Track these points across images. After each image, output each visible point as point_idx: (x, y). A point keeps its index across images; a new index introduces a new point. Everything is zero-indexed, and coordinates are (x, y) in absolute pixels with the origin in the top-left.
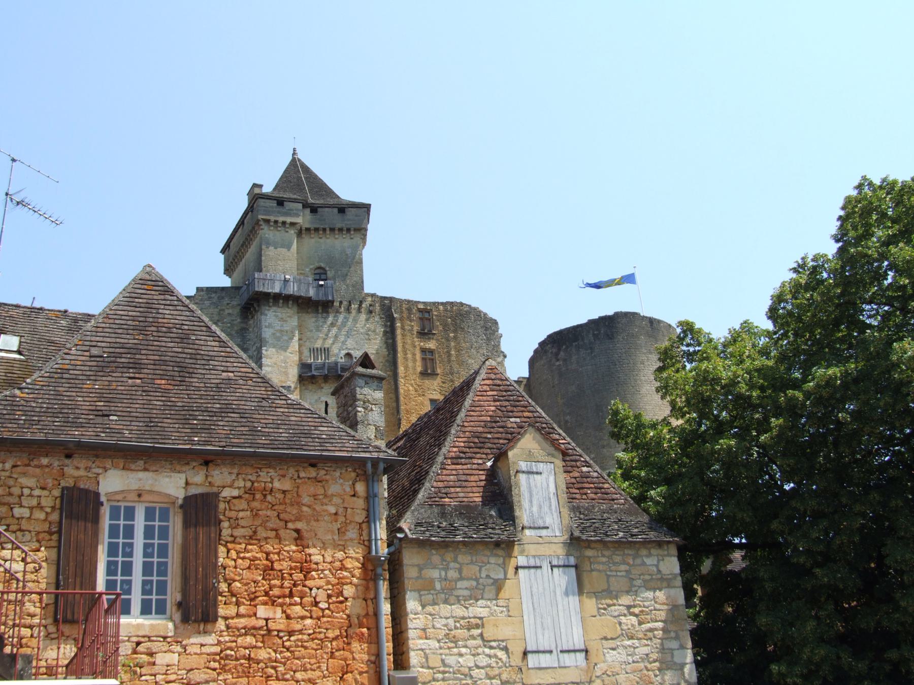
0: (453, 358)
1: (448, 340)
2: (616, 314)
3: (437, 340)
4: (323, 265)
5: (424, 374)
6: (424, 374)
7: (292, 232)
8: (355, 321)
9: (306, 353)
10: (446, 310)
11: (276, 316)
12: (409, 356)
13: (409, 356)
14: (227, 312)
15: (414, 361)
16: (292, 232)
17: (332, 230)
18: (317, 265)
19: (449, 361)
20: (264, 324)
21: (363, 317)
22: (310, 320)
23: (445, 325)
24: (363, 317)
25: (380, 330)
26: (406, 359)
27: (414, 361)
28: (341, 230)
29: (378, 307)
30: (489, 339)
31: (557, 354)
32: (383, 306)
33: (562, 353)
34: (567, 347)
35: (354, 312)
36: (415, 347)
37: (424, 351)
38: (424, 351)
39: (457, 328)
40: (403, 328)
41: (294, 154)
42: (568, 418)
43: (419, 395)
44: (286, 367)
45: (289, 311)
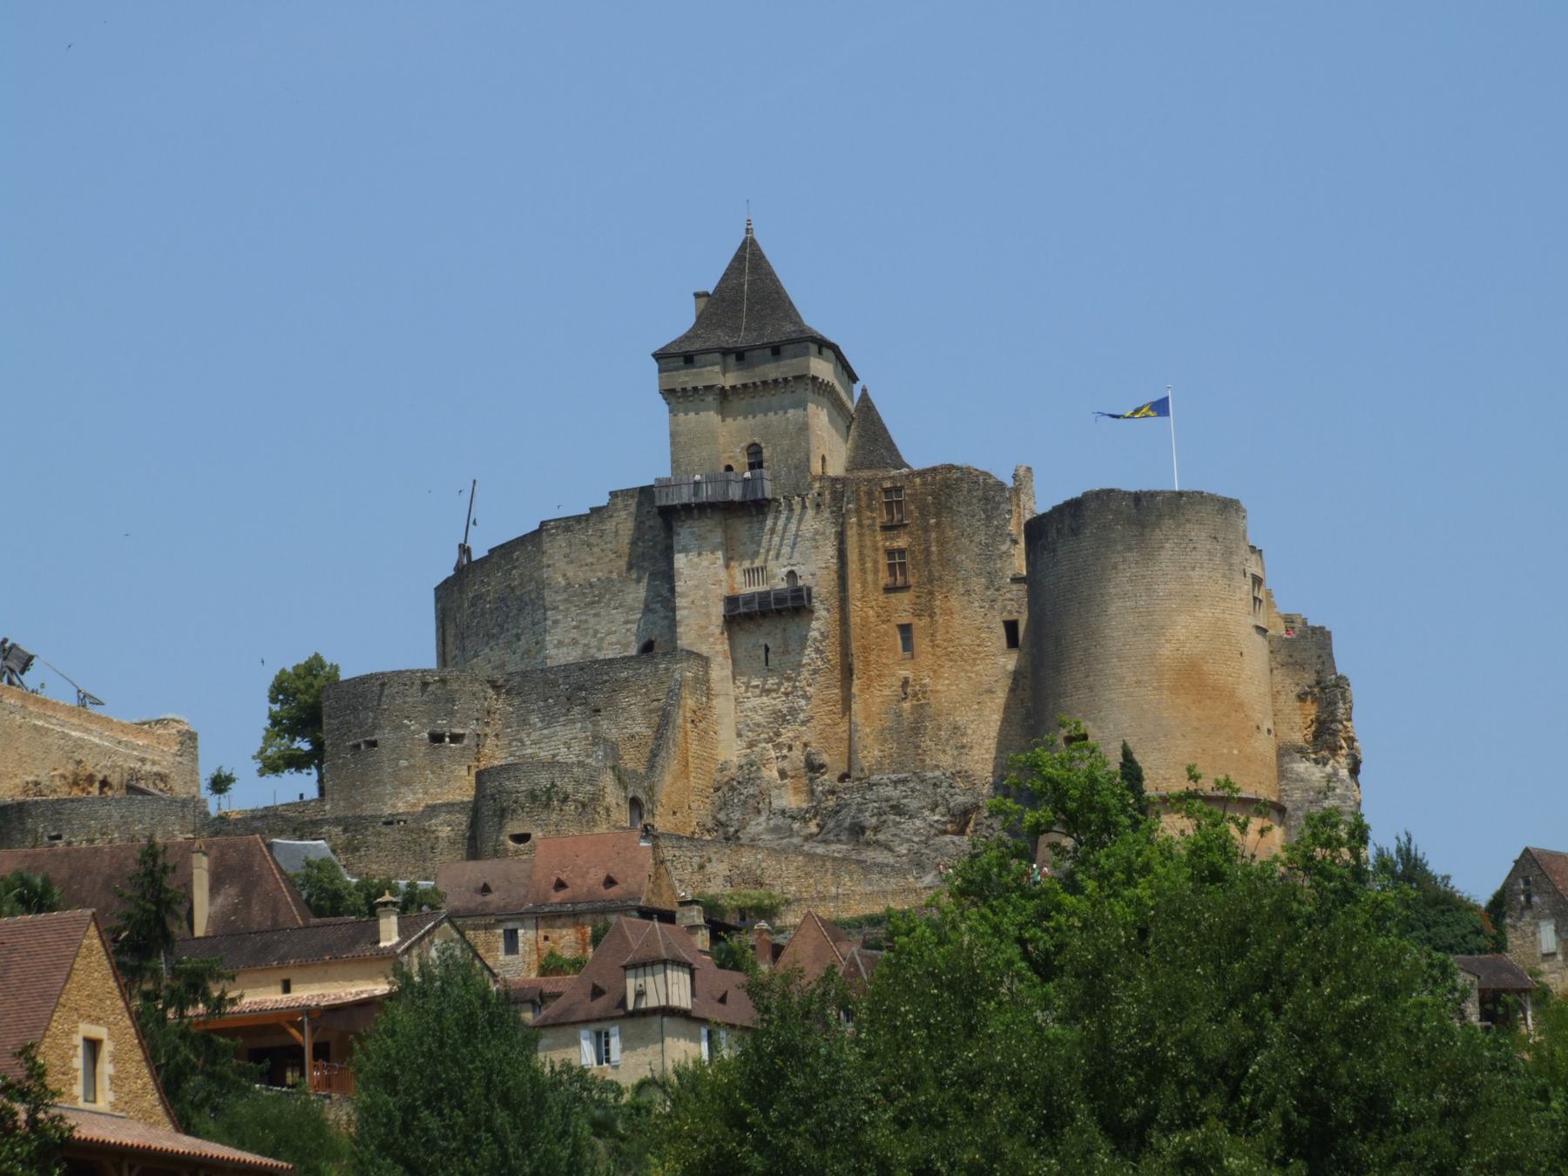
0: (934, 558)
2: (1085, 495)
3: (911, 533)
4: (757, 440)
5: (888, 590)
7: (711, 398)
8: (800, 521)
10: (924, 484)
11: (692, 533)
12: (869, 565)
13: (869, 565)
15: (876, 571)
16: (711, 398)
18: (749, 441)
19: (927, 562)
21: (810, 513)
22: (742, 528)
24: (810, 513)
25: (831, 530)
26: (863, 571)
27: (876, 571)
28: (775, 381)
30: (989, 518)
35: (797, 508)
36: (877, 549)
37: (890, 553)
38: (890, 553)
39: (941, 508)
40: (860, 525)
43: (883, 622)
44: (707, 606)
45: (710, 522)
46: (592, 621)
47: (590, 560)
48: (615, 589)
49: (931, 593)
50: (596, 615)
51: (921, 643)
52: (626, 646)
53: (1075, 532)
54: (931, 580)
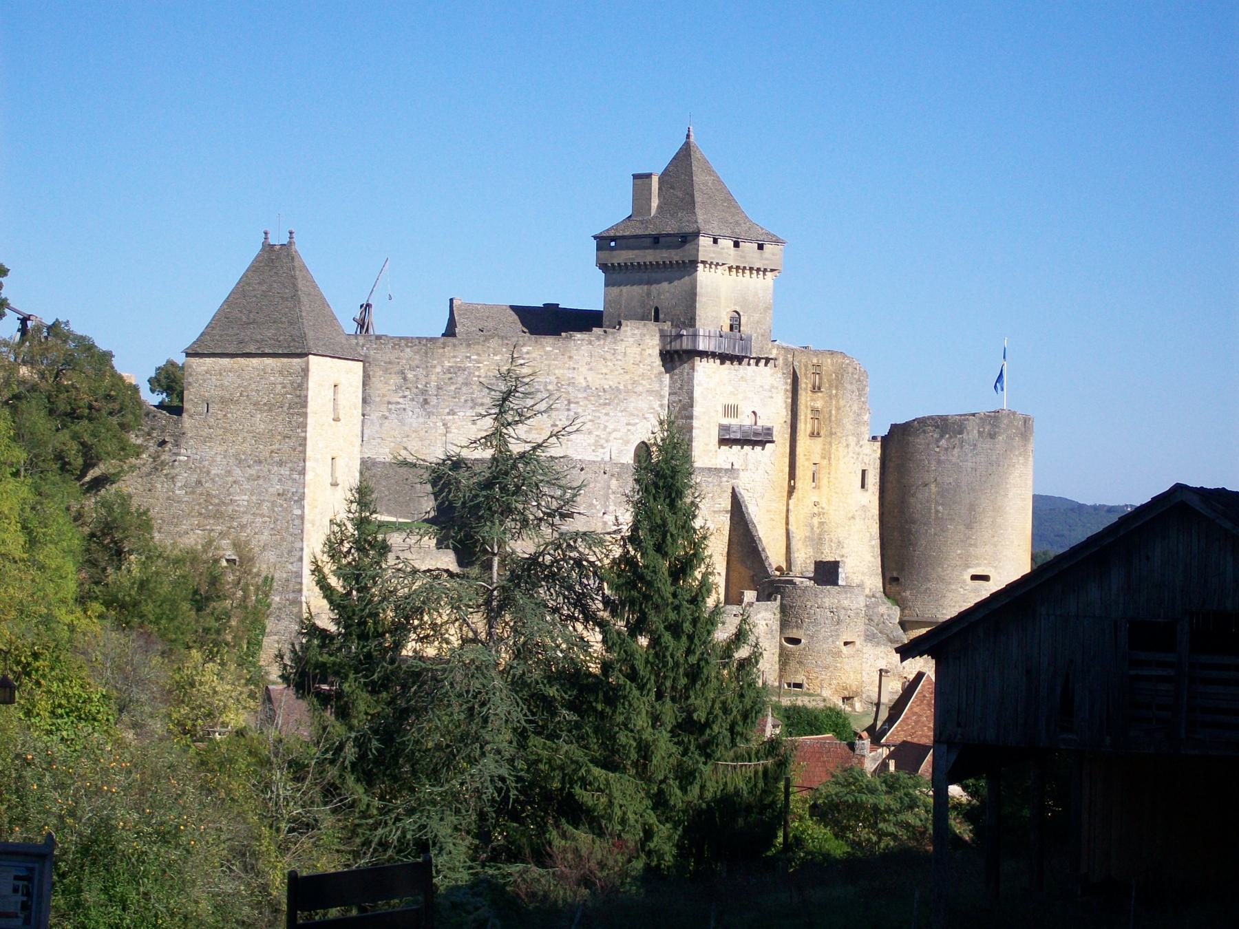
1: (831, 397)
5: (812, 435)
6: (812, 435)
9: (721, 410)
14: (650, 351)
17: (751, 269)
20: (696, 382)
23: (830, 381)
29: (780, 362)
31: (938, 441)
32: (786, 359)
33: (943, 442)
34: (951, 437)
38: (815, 411)
41: (688, 136)
42: (940, 508)
44: (709, 429)
46: (604, 418)
47: (604, 371)
48: (621, 397)
49: (830, 443)
50: (607, 414)
51: (824, 481)
52: (627, 442)
53: (992, 436)
54: (831, 434)
